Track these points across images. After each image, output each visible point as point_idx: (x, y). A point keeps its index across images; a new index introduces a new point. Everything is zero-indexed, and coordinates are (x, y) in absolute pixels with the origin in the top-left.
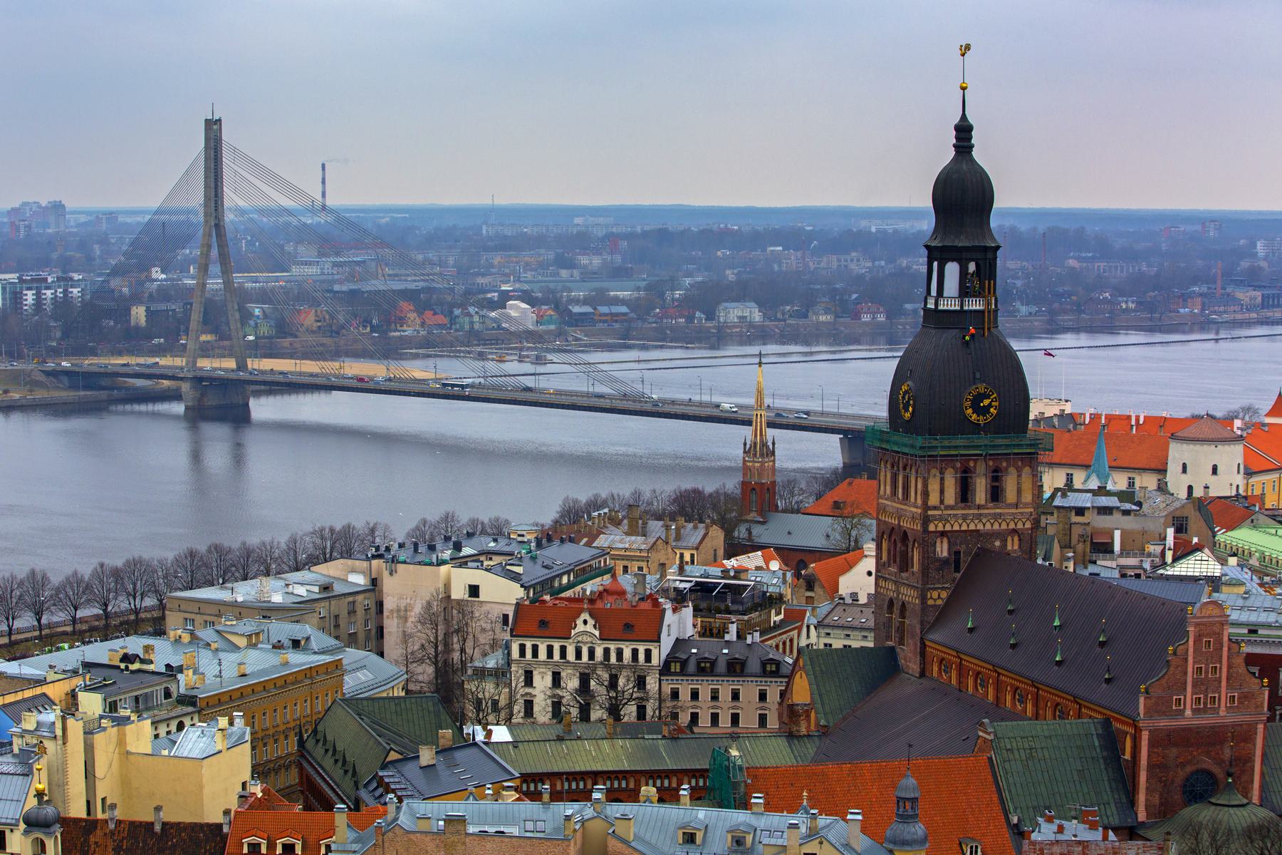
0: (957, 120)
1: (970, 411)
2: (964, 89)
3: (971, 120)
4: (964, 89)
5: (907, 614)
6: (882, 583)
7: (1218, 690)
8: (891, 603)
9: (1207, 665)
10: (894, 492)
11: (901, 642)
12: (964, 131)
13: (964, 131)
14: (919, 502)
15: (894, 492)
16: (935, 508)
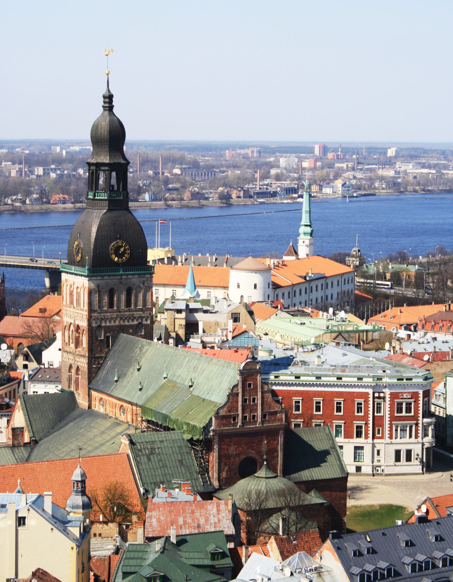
0: (104, 91)
1: (113, 256)
2: (108, 75)
3: (113, 92)
4: (108, 75)
5: (80, 373)
6: (65, 355)
7: (256, 410)
8: (71, 367)
9: (250, 397)
10: (72, 303)
11: (77, 388)
12: (109, 99)
13: (109, 99)
14: (86, 308)
15: (72, 303)
16: (95, 311)
